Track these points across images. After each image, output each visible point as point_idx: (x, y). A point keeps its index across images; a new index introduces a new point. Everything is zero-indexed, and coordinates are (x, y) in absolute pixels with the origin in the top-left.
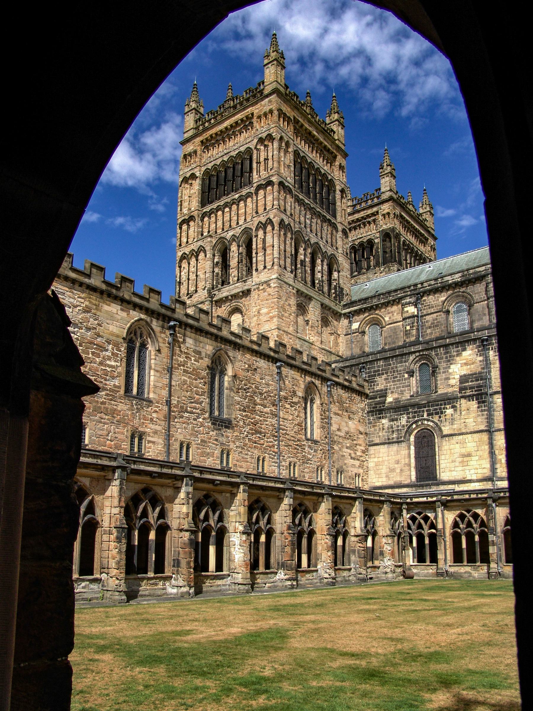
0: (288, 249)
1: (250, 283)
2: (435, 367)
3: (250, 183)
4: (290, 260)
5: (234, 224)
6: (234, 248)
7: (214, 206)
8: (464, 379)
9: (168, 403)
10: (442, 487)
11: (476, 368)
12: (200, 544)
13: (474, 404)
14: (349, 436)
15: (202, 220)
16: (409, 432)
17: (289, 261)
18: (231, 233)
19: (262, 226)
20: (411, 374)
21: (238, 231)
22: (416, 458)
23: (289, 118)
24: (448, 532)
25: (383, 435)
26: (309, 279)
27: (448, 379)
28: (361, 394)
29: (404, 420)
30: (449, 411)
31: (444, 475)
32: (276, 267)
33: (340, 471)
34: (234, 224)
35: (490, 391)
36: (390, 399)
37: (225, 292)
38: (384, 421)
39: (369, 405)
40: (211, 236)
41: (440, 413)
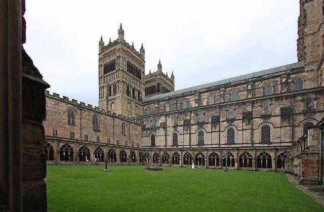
1: (116, 96)
2: (156, 120)
7: (109, 74)
8: (161, 123)
11: (164, 121)
14: (135, 135)
16: (150, 135)
17: (125, 91)
26: (132, 96)
31: (156, 145)
33: (133, 143)
37: (110, 98)
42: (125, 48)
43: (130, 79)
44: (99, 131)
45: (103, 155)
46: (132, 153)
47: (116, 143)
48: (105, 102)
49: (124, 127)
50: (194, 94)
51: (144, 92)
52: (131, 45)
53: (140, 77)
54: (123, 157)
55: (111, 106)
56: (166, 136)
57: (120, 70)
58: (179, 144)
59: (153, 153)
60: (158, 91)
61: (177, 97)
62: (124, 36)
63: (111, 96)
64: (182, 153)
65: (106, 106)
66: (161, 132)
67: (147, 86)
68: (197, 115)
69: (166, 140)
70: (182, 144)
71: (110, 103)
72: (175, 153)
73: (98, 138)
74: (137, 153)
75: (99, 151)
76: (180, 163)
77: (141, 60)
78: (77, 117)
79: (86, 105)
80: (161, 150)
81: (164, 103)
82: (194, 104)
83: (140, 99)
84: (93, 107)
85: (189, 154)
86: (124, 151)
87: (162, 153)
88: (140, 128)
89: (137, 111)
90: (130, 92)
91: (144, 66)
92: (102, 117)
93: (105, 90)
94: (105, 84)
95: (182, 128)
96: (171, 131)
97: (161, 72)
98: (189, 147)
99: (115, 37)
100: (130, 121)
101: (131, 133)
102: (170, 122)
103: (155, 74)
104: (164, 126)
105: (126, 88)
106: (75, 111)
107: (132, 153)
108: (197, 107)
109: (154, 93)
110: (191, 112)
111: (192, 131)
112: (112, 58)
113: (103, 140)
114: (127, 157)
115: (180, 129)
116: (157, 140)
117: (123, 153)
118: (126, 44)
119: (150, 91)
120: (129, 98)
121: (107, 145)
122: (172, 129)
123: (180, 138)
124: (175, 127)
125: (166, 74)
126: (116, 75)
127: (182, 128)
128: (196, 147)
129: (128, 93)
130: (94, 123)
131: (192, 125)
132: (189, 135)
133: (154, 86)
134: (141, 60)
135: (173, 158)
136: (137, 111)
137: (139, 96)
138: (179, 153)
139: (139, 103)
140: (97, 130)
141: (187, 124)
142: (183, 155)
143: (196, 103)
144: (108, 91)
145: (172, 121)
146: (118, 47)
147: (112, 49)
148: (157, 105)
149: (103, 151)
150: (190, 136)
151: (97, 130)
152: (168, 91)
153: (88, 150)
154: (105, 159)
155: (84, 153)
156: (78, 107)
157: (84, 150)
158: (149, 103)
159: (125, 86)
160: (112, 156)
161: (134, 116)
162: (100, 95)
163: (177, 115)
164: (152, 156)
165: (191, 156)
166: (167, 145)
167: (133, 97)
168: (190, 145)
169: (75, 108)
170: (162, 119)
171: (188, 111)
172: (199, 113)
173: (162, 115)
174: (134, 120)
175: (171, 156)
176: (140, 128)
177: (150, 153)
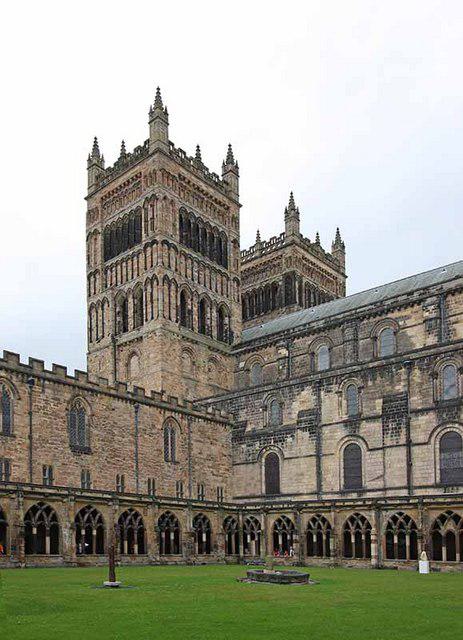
0: (173, 301)
2: (282, 404)
4: (175, 311)
5: (130, 277)
6: (130, 300)
7: (118, 258)
9: (30, 437)
10: (283, 499)
11: (311, 405)
12: (457, 539)
13: (307, 434)
15: (106, 273)
16: (260, 455)
17: (173, 312)
18: (127, 286)
19: (151, 280)
20: (265, 408)
21: (132, 285)
22: (266, 481)
25: (243, 457)
27: (290, 413)
28: (223, 424)
30: (289, 440)
31: (284, 490)
32: (160, 318)
34: (130, 277)
35: (320, 424)
36: (249, 429)
38: (243, 446)
39: (233, 433)
40: (112, 289)
41: (282, 440)
42: (173, 168)
43: (188, 269)
44: (88, 451)
45: (101, 530)
46: (201, 523)
47: (144, 489)
48: (109, 353)
49: (173, 432)
50: (419, 302)
51: (237, 311)
52: (191, 153)
53: (223, 260)
54: (168, 536)
55: (128, 365)
56: (318, 456)
57: (155, 242)
58: (367, 484)
59: (272, 521)
60: (289, 302)
61: (355, 318)
62: (170, 129)
63: (125, 330)
64: (378, 517)
65: (110, 365)
66: (301, 443)
67: (248, 288)
68: (435, 375)
69: (319, 474)
70: (379, 484)
71: (123, 355)
72: (352, 519)
73: (85, 475)
74: (215, 521)
75: (89, 520)
76: (373, 553)
77: (226, 200)
78: (19, 407)
79: (48, 367)
80: (300, 507)
81: (309, 340)
82: (419, 338)
83: (225, 335)
84: (71, 373)
85: (407, 519)
86: (173, 517)
87: (306, 518)
89: (214, 374)
90: (191, 312)
91: (236, 221)
92: (100, 404)
93: (109, 313)
94: (108, 295)
95: (377, 426)
96: (335, 438)
97: (296, 232)
98: (404, 493)
99: (138, 134)
100: (190, 412)
101: (195, 451)
102: (333, 407)
103: (277, 244)
104: (312, 423)
105: (175, 301)
106: (15, 390)
107: (201, 523)
108: (434, 346)
109: (274, 309)
110: (410, 366)
111: (418, 436)
112: (129, 207)
113: (103, 482)
114: (183, 536)
115: (372, 430)
116: (287, 471)
117: (167, 523)
118: (174, 154)
119: (259, 304)
120: (185, 332)
121: (117, 496)
122: (341, 433)
123: (370, 463)
124: (353, 423)
125: (313, 241)
126: (142, 261)
127: (377, 426)
128: (431, 492)
130: (72, 425)
131: (417, 412)
132: (404, 450)
133: (275, 287)
134: (226, 200)
135: (347, 536)
136: (214, 374)
137: (221, 326)
138: (370, 516)
139: (221, 347)
140: (81, 449)
141: (396, 413)
142: (385, 523)
143: (429, 331)
144: (117, 314)
145: (340, 405)
147: (130, 175)
148: (284, 352)
149: (101, 520)
150: (409, 454)
151: (81, 449)
152: (324, 298)
153: (55, 518)
154: (107, 545)
155: (41, 528)
156: (23, 374)
157: (41, 518)
158: (257, 344)
160: (132, 534)
161: (206, 392)
162: (90, 330)
163: (358, 381)
164: (270, 532)
165: (414, 526)
166: (325, 488)
167: (202, 330)
168: (409, 487)
169: (14, 380)
170: (305, 399)
171: (399, 365)
172: (439, 368)
173: (302, 385)
174: (207, 406)
175: (340, 530)
176: (225, 434)
177: (261, 519)
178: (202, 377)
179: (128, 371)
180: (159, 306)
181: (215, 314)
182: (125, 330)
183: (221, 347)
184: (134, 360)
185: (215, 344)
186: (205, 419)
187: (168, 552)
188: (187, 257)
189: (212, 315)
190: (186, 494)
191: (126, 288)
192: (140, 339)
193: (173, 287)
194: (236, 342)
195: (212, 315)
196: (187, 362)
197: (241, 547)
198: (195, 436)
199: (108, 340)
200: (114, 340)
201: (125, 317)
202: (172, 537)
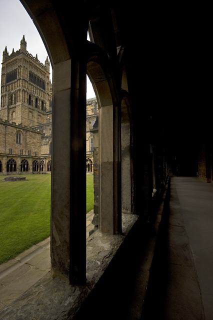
0: (26, 97)
3: (16, 78)
17: (26, 100)
23: (28, 62)
24: (47, 164)
29: (47, 140)
48: (6, 110)
49: (20, 135)
53: (44, 88)
55: (12, 115)
59: (47, 161)
63: (12, 104)
65: (6, 114)
71: (11, 111)
74: (30, 162)
77: (45, 71)
88: (39, 137)
90: (32, 101)
93: (7, 99)
101: (28, 141)
105: (27, 97)
120: (30, 106)
129: (30, 102)
134: (45, 71)
136: (40, 120)
144: (9, 99)
146: (20, 56)
159: (26, 95)
162: (1, 103)
167: (36, 106)
177: (44, 160)
178: (36, 120)
179: (12, 117)
180: (21, 98)
181: (41, 103)
182: (12, 104)
183: (42, 112)
184: (14, 113)
185: (40, 111)
186: (32, 132)
187: (11, 171)
188: (31, 85)
189: (40, 103)
190: (24, 153)
191: (12, 92)
192: (16, 107)
193: (26, 93)
194: (47, 111)
195: (40, 103)
196: (31, 115)
197: (39, 169)
198: (28, 137)
199: (6, 106)
200: (8, 107)
201: (12, 100)
202: (13, 166)
